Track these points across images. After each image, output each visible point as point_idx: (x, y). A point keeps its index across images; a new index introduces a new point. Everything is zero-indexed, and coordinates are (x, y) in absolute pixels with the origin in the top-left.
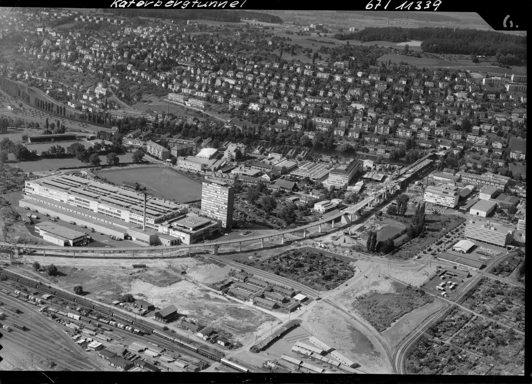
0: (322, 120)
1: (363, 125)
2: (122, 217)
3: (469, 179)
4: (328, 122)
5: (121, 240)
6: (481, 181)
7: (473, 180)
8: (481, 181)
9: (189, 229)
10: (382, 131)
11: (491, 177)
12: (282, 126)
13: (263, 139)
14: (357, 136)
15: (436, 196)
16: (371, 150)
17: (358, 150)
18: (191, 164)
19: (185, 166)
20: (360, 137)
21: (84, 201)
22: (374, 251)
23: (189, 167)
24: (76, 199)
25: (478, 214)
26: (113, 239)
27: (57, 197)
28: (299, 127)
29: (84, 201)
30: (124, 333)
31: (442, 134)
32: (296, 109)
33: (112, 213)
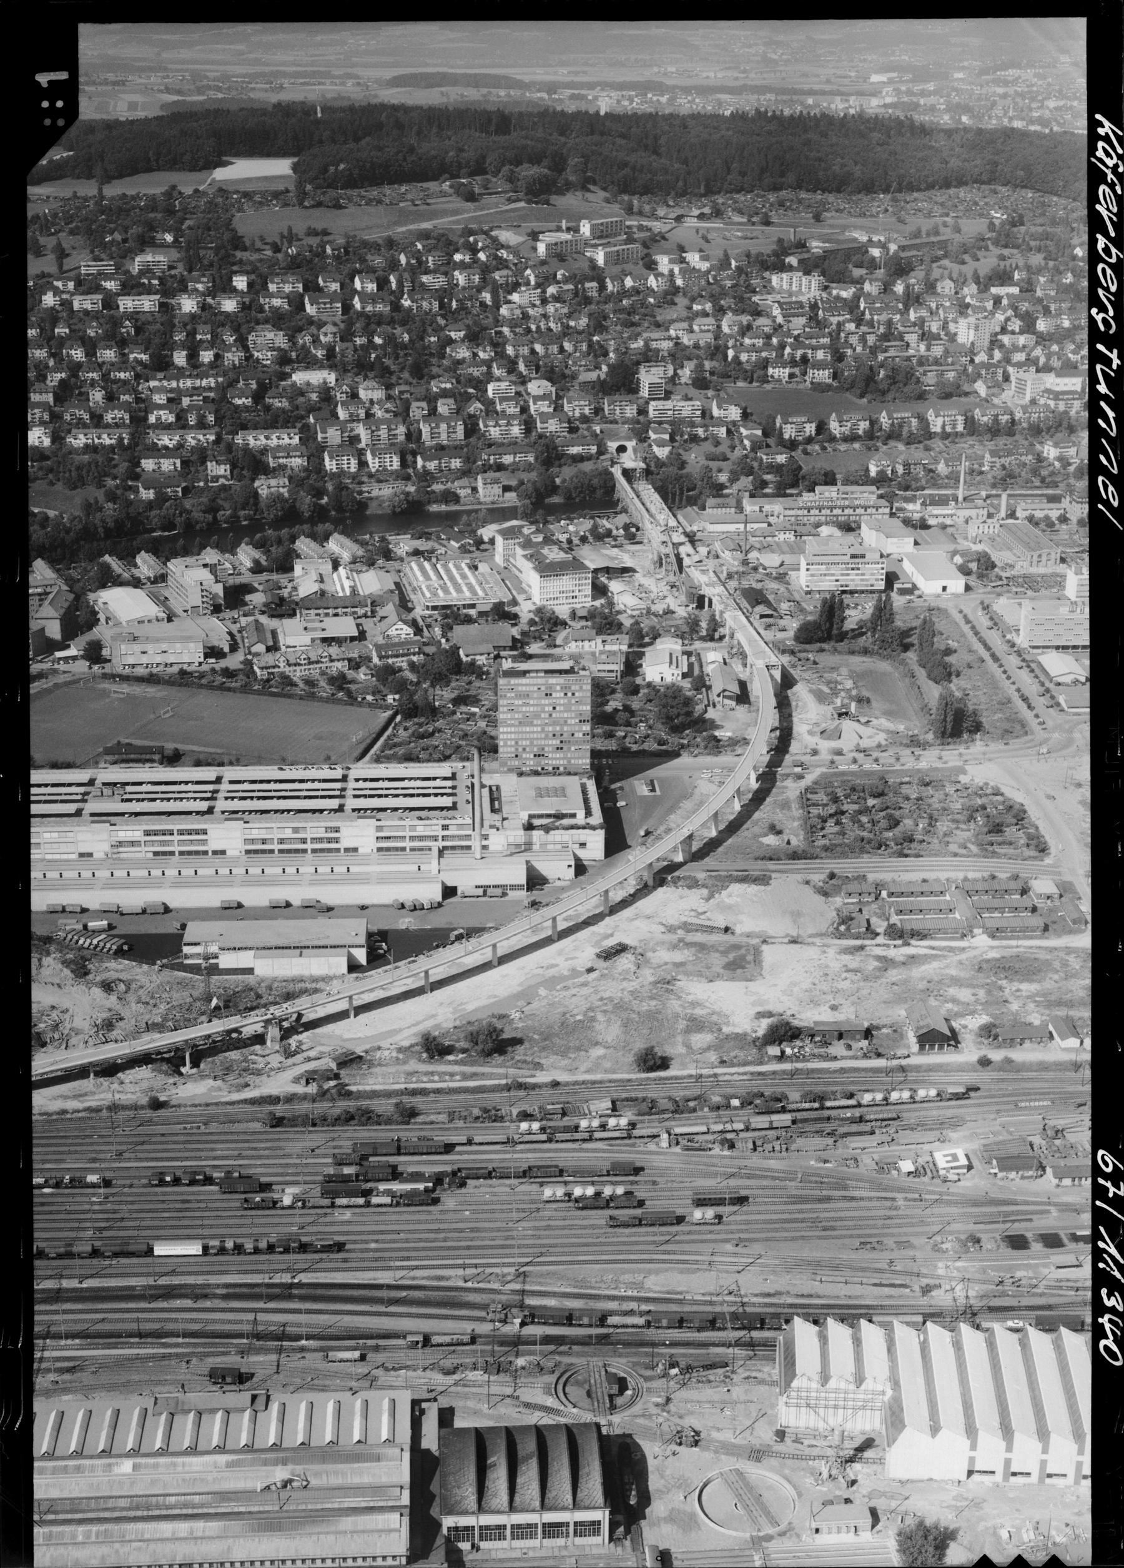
0: (267, 438)
1: (390, 430)
2: (345, 843)
3: (800, 512)
4: (287, 441)
5: (440, 905)
6: (831, 509)
7: (812, 512)
8: (831, 509)
9: (573, 816)
10: (444, 436)
11: (834, 495)
12: (156, 482)
13: (154, 530)
14: (396, 463)
15: (836, 570)
16: (462, 493)
17: (429, 503)
18: (164, 647)
19: (144, 660)
20: (404, 463)
21: (181, 832)
22: (952, 735)
23: (159, 659)
24: (147, 833)
25: (944, 588)
26: (415, 909)
27: (63, 848)
28: (222, 472)
29: (181, 832)
30: (915, 1110)
31: (587, 411)
32: (158, 419)
33: (304, 841)
